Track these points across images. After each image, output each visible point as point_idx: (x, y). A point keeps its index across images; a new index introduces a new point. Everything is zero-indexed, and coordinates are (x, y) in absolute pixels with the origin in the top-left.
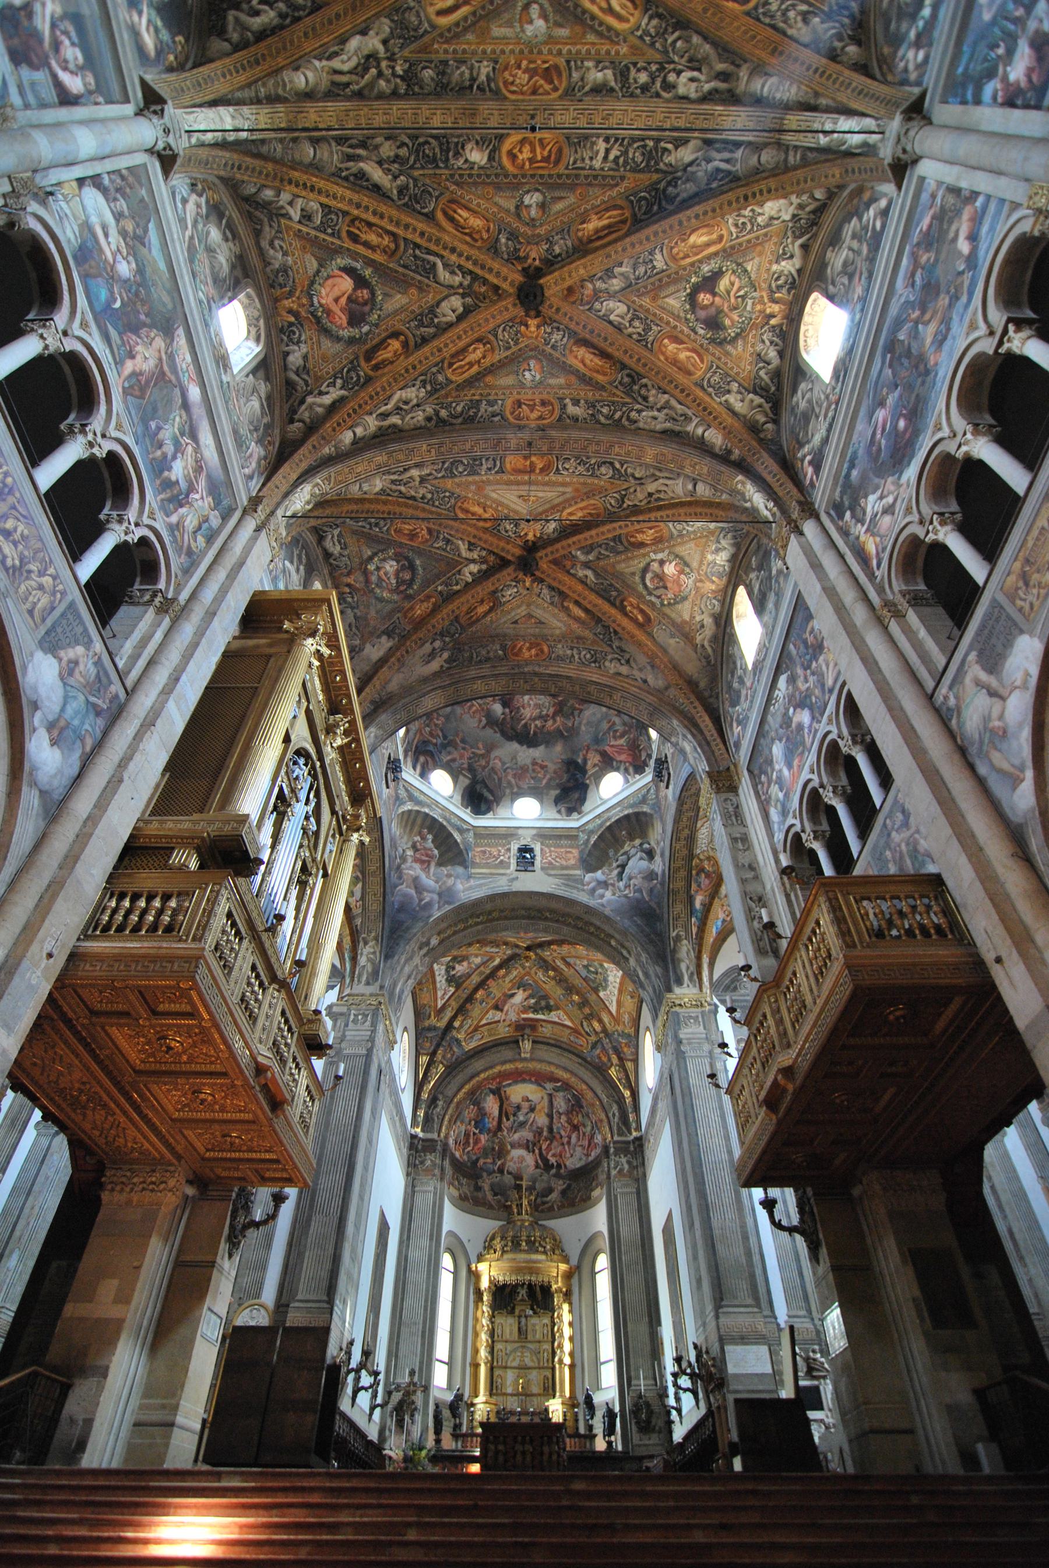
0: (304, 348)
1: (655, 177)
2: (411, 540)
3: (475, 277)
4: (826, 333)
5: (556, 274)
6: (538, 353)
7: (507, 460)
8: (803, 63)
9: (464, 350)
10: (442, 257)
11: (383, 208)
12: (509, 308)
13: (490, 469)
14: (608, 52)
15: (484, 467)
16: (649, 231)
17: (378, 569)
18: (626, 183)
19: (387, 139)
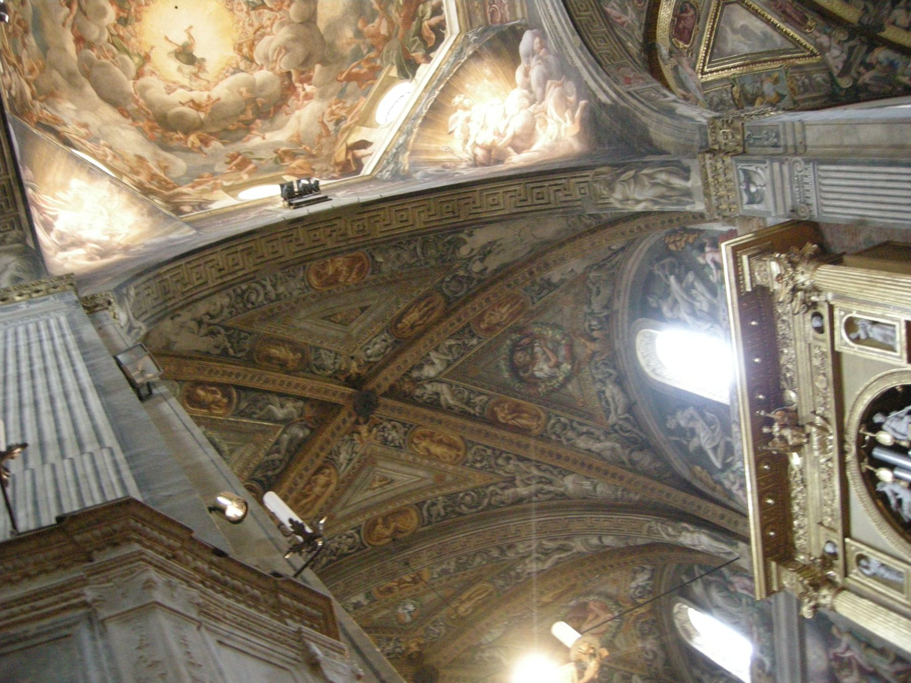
0: (633, 584)
2: (518, 405)
7: (416, 521)
13: (434, 504)
15: (440, 506)
17: (558, 365)
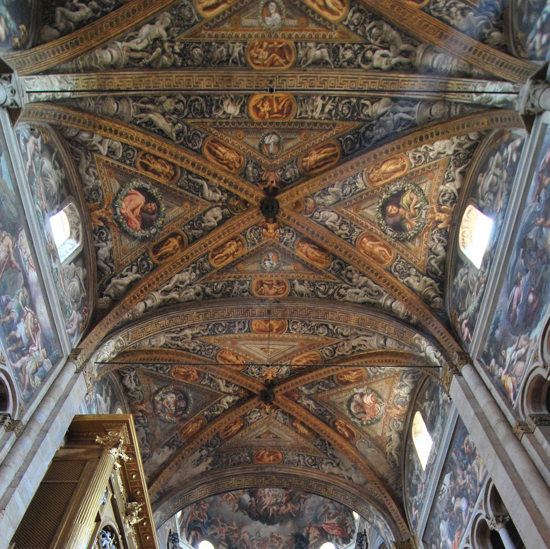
1: (357, 124)
3: (231, 195)
4: (478, 234)
5: (288, 192)
6: (274, 247)
8: (461, 44)
9: (223, 246)
10: (207, 180)
11: (165, 146)
12: (255, 216)
14: (324, 37)
16: (353, 162)
18: (336, 129)
19: (169, 97)
